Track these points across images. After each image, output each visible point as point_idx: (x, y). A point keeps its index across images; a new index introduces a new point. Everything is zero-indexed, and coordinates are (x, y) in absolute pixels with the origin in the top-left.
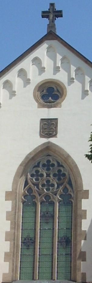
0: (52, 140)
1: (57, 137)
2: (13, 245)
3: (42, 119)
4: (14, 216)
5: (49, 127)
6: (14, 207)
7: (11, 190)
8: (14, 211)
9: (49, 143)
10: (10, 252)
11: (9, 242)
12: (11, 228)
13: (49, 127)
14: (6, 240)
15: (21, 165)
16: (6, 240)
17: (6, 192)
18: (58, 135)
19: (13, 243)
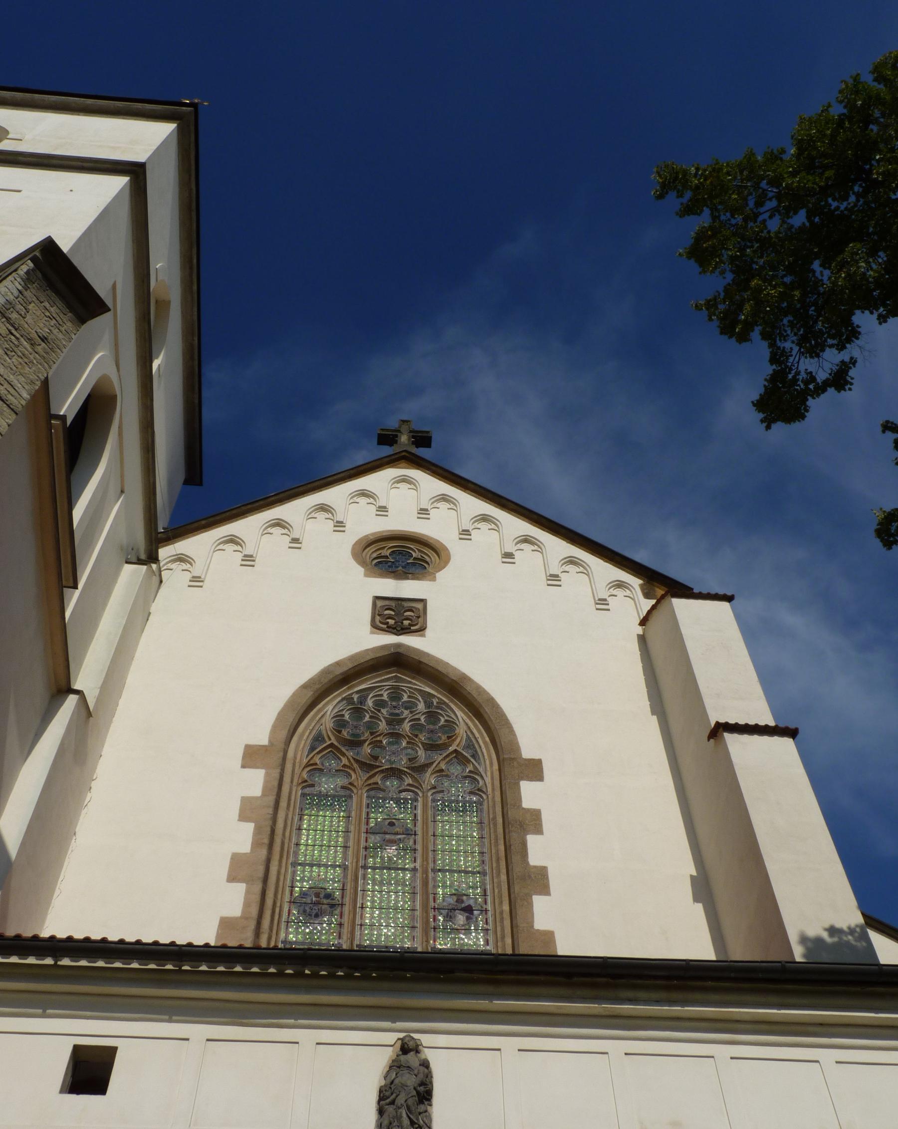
0: (410, 641)
1: (423, 636)
2: (257, 898)
3: (377, 598)
4: (271, 811)
5: (398, 616)
6: (276, 790)
7: (265, 741)
8: (271, 799)
9: (399, 645)
10: (245, 917)
11: (240, 889)
12: (256, 844)
13: (398, 616)
14: (232, 878)
15: (305, 687)
16: (232, 878)
17: (248, 748)
18: (428, 632)
19: (258, 887)
